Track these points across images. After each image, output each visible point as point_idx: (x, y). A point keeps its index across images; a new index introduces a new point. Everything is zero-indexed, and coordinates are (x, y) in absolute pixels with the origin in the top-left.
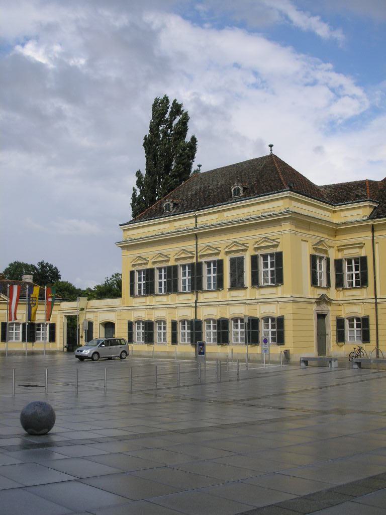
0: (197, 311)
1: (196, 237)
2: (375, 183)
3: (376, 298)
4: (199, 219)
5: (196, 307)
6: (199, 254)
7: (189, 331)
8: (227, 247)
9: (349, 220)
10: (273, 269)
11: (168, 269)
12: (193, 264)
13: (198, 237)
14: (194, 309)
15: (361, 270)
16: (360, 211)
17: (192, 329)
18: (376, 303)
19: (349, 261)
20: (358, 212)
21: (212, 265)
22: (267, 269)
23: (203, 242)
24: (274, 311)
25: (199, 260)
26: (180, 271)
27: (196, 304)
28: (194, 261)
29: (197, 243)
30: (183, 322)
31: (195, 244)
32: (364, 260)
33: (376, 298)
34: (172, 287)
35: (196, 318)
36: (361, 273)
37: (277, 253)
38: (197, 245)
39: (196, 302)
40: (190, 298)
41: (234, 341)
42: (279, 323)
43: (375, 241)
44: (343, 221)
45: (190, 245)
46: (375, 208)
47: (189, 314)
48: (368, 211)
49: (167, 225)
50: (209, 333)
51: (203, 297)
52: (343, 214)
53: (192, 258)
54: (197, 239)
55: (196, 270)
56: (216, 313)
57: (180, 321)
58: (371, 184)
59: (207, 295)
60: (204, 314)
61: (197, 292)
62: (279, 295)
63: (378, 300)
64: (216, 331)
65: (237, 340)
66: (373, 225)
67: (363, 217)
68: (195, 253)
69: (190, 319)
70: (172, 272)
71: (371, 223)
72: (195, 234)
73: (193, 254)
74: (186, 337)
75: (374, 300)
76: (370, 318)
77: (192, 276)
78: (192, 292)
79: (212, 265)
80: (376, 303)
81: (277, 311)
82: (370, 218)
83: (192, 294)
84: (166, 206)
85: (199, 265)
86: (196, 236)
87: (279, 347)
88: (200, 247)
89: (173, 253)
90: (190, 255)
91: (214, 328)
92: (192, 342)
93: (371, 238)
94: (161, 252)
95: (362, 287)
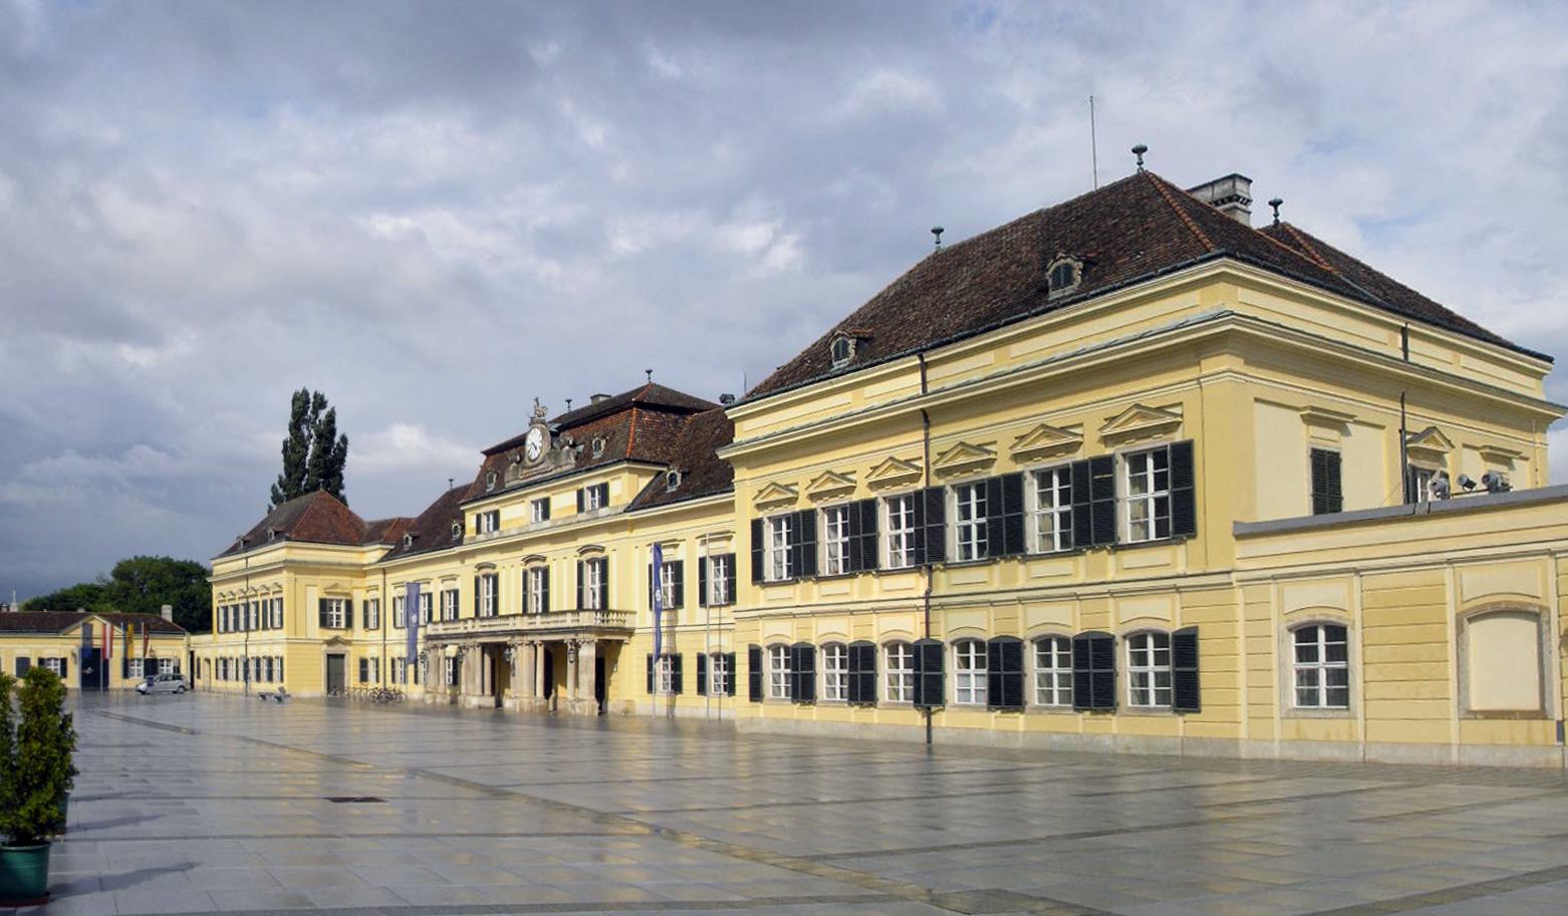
0: (931, 619)
1: (927, 420)
4: (931, 374)
5: (928, 608)
6: (933, 468)
7: (911, 671)
8: (1021, 438)
10: (1163, 493)
11: (851, 511)
12: (918, 494)
13: (930, 418)
14: (924, 613)
17: (917, 668)
21: (973, 493)
22: (1143, 496)
23: (946, 435)
24: (1168, 614)
25: (936, 482)
26: (884, 514)
27: (927, 602)
28: (921, 485)
29: (927, 435)
30: (893, 647)
31: (923, 437)
34: (862, 557)
35: (928, 635)
37: (1176, 447)
38: (927, 441)
39: (927, 597)
40: (917, 584)
41: (1040, 702)
42: (1183, 648)
45: (908, 445)
47: (911, 628)
49: (847, 396)
50: (963, 682)
51: (947, 582)
53: (914, 478)
54: (927, 428)
55: (926, 509)
56: (986, 625)
57: (884, 645)
59: (958, 576)
60: (948, 627)
61: (930, 568)
62: (1180, 570)
64: (985, 671)
65: (1049, 697)
68: (921, 464)
69: (912, 639)
70: (860, 519)
72: (923, 410)
73: (917, 468)
74: (902, 685)
77: (916, 525)
78: (918, 569)
79: (973, 493)
81: (1174, 616)
83: (918, 574)
84: (836, 347)
85: (936, 496)
86: (926, 418)
87: (1180, 719)
88: (937, 447)
89: (861, 468)
90: (912, 471)
91: (980, 663)
92: (917, 700)
94: (774, 479)
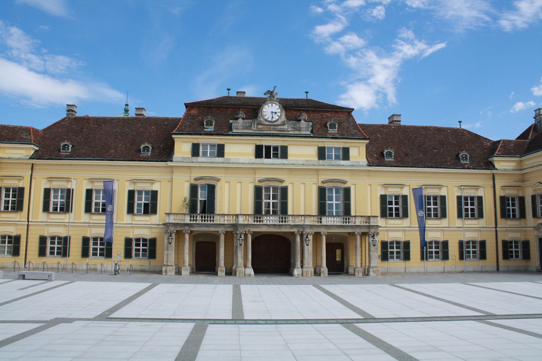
2: (37, 131)
3: (28, 221)
9: (13, 156)
15: (18, 197)
16: (24, 152)
18: (28, 225)
19: (8, 190)
20: (24, 151)
32: (22, 190)
33: (28, 221)
36: (18, 200)
43: (33, 177)
44: (7, 156)
46: (37, 151)
48: (32, 152)
52: (7, 151)
58: (36, 131)
63: (30, 223)
66: (33, 164)
67: (26, 156)
71: (33, 161)
75: (27, 223)
76: (22, 237)
80: (28, 225)
82: (31, 158)
93: (30, 174)
95: (65, 213)
